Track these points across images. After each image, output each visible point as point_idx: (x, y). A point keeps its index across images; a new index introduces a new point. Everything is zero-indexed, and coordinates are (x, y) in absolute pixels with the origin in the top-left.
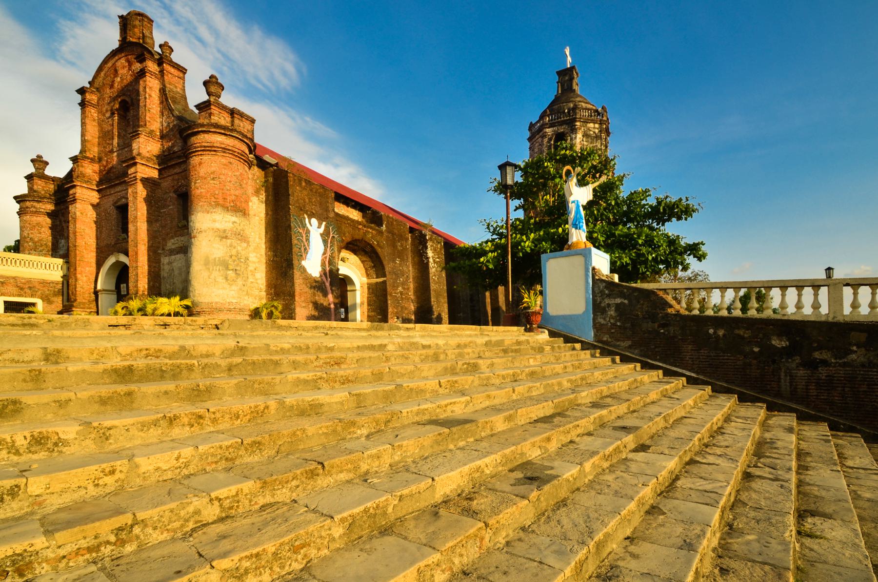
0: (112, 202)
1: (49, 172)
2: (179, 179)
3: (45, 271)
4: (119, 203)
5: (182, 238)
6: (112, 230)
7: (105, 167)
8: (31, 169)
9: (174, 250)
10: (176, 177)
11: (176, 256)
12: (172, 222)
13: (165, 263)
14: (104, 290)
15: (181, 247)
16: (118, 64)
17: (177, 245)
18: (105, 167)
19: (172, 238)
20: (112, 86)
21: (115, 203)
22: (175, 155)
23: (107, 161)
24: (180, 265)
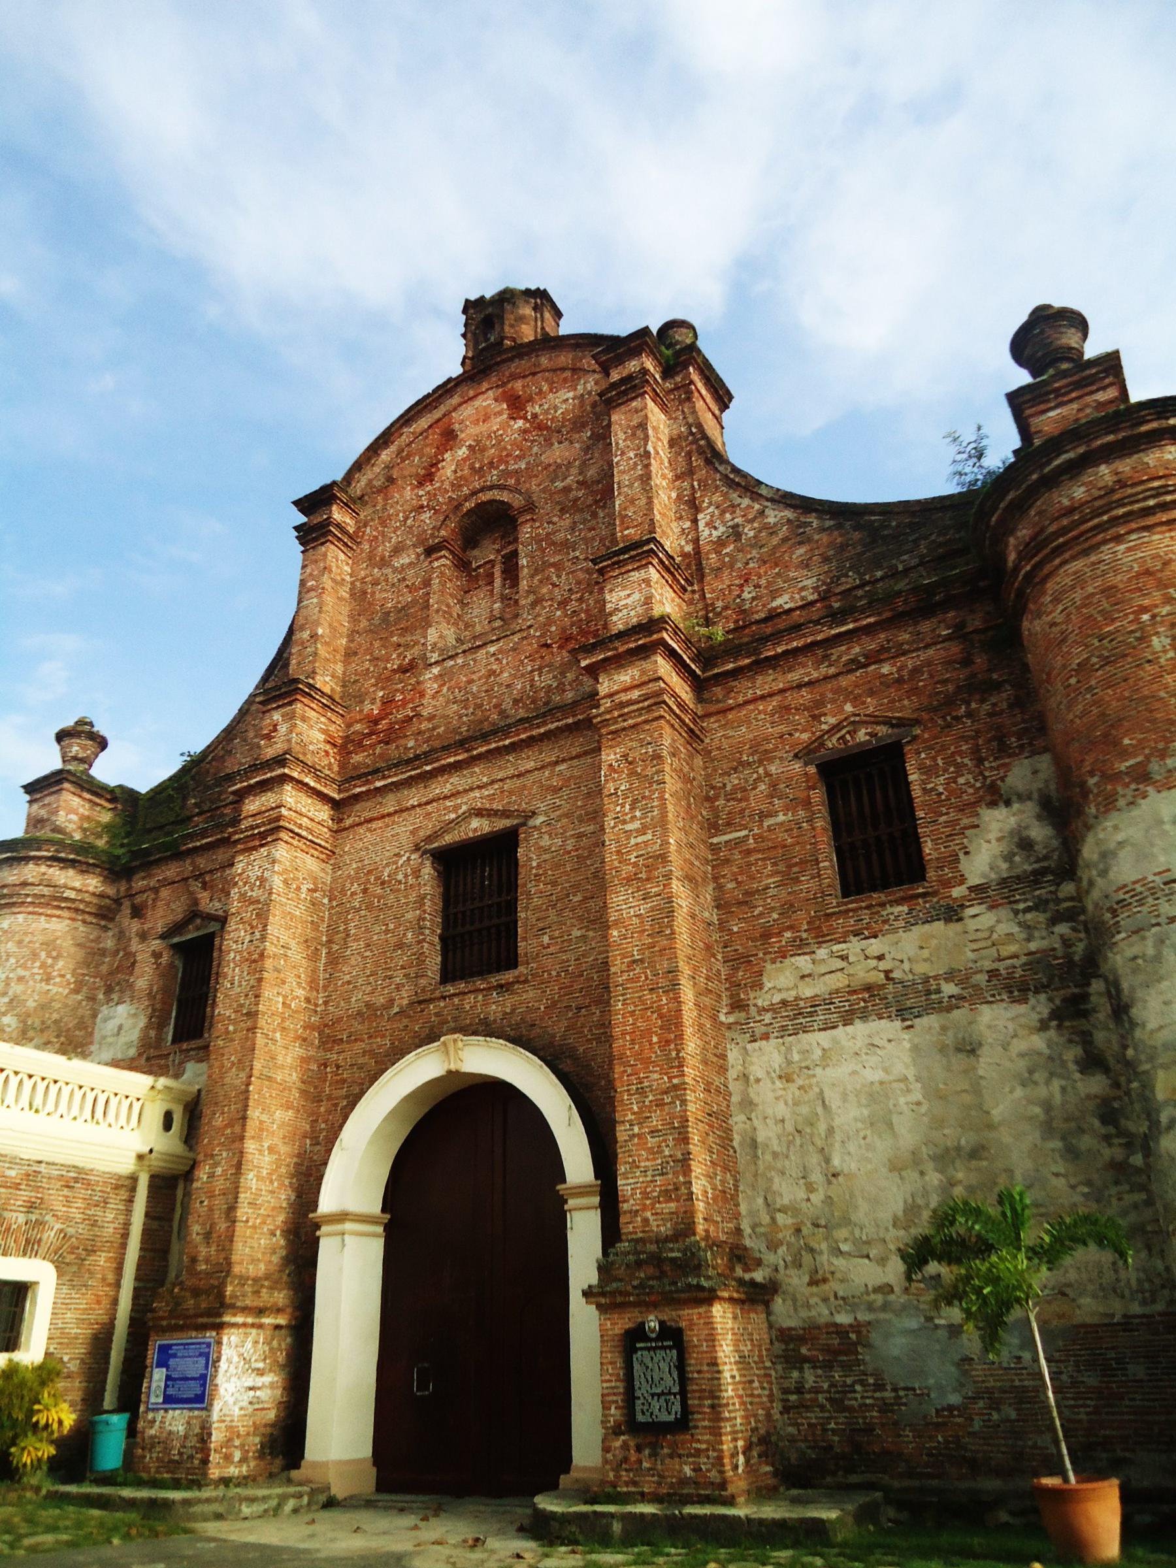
0: (406, 840)
1: (106, 770)
2: (820, 703)
3: (91, 1125)
4: (448, 839)
5: (875, 946)
6: (400, 945)
7: (376, 722)
8: (50, 760)
9: (815, 1003)
10: (806, 695)
11: (840, 1032)
12: (790, 879)
13: (756, 1071)
14: (341, 1217)
15: (868, 988)
16: (468, 411)
17: (838, 981)
18: (376, 722)
19: (800, 947)
20: (429, 477)
21: (429, 839)
22: (782, 624)
23: (387, 702)
24: (873, 1075)
